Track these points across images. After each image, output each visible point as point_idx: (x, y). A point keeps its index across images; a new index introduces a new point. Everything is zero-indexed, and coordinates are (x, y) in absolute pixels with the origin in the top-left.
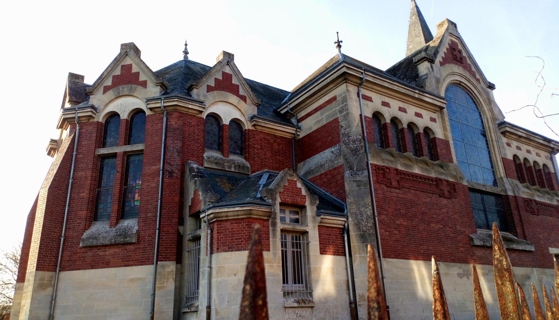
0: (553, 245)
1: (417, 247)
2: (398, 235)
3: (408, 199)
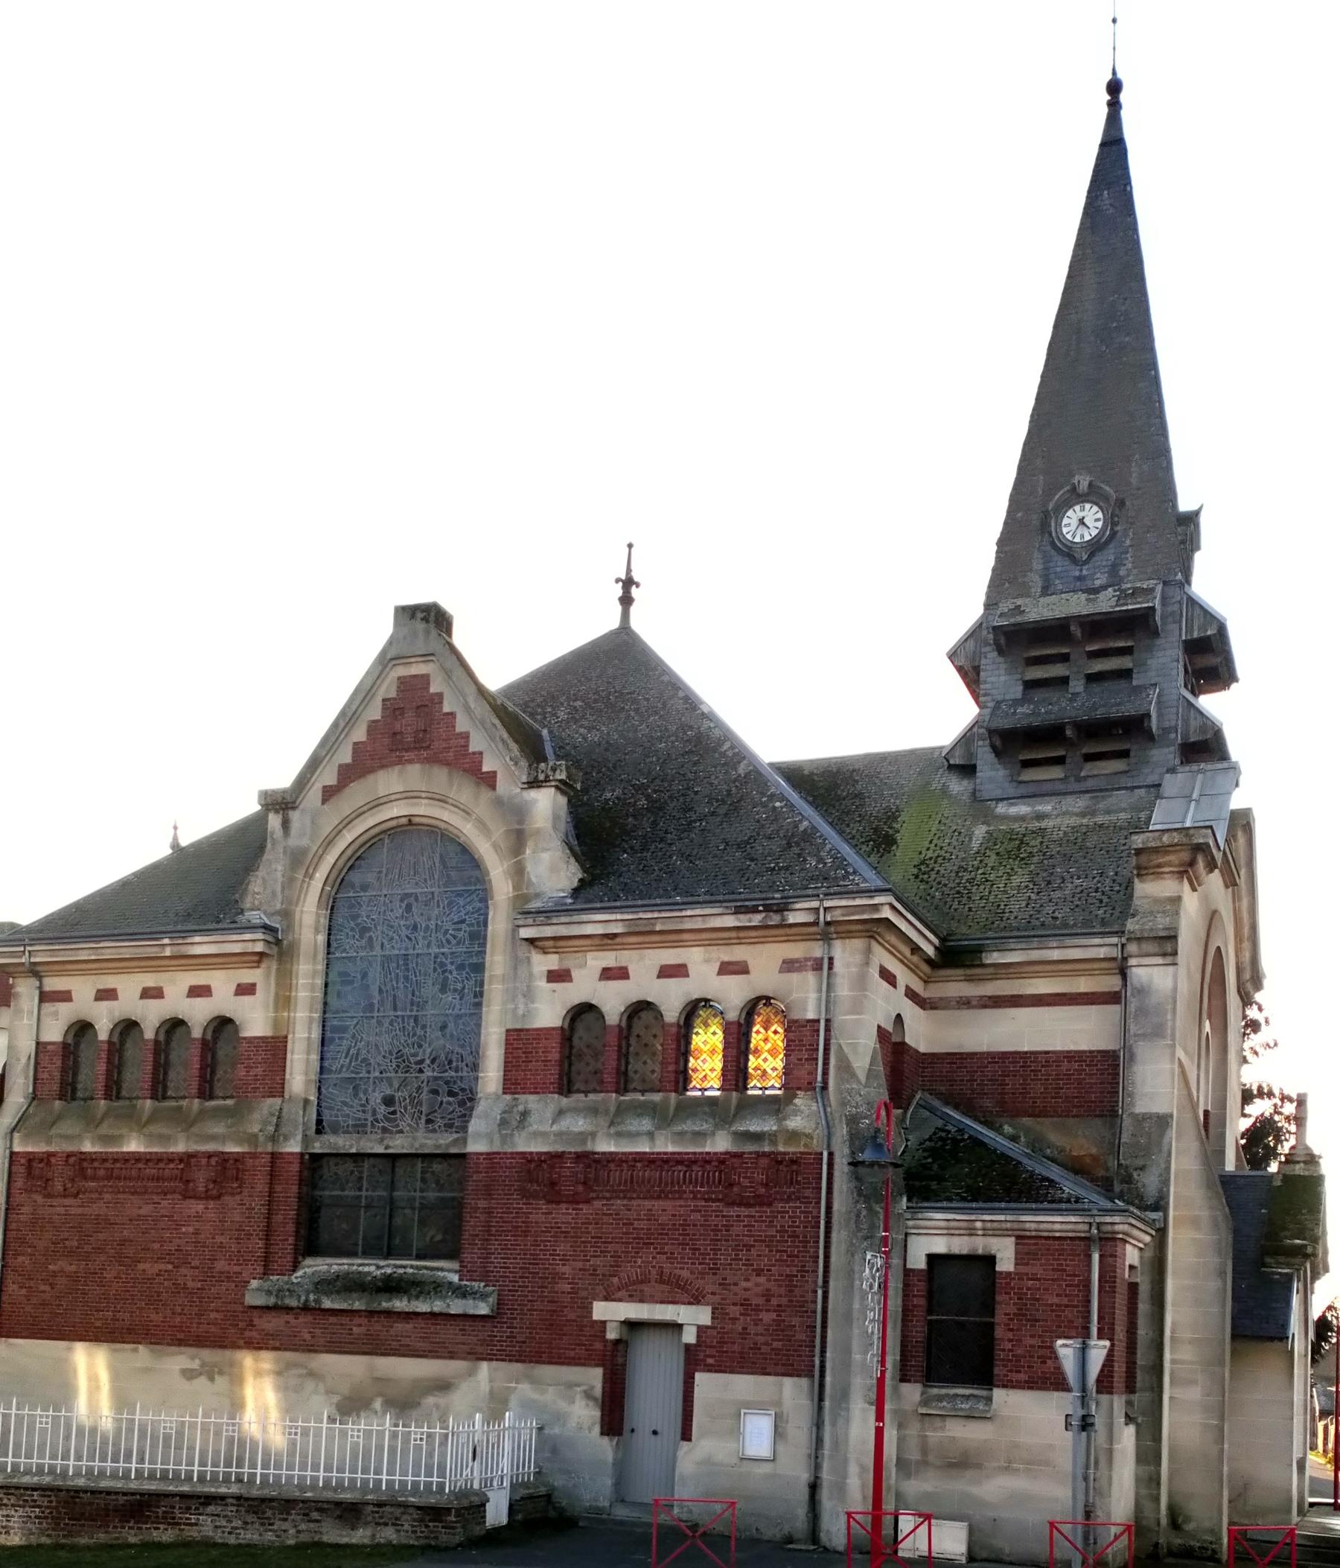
0: (620, 1294)
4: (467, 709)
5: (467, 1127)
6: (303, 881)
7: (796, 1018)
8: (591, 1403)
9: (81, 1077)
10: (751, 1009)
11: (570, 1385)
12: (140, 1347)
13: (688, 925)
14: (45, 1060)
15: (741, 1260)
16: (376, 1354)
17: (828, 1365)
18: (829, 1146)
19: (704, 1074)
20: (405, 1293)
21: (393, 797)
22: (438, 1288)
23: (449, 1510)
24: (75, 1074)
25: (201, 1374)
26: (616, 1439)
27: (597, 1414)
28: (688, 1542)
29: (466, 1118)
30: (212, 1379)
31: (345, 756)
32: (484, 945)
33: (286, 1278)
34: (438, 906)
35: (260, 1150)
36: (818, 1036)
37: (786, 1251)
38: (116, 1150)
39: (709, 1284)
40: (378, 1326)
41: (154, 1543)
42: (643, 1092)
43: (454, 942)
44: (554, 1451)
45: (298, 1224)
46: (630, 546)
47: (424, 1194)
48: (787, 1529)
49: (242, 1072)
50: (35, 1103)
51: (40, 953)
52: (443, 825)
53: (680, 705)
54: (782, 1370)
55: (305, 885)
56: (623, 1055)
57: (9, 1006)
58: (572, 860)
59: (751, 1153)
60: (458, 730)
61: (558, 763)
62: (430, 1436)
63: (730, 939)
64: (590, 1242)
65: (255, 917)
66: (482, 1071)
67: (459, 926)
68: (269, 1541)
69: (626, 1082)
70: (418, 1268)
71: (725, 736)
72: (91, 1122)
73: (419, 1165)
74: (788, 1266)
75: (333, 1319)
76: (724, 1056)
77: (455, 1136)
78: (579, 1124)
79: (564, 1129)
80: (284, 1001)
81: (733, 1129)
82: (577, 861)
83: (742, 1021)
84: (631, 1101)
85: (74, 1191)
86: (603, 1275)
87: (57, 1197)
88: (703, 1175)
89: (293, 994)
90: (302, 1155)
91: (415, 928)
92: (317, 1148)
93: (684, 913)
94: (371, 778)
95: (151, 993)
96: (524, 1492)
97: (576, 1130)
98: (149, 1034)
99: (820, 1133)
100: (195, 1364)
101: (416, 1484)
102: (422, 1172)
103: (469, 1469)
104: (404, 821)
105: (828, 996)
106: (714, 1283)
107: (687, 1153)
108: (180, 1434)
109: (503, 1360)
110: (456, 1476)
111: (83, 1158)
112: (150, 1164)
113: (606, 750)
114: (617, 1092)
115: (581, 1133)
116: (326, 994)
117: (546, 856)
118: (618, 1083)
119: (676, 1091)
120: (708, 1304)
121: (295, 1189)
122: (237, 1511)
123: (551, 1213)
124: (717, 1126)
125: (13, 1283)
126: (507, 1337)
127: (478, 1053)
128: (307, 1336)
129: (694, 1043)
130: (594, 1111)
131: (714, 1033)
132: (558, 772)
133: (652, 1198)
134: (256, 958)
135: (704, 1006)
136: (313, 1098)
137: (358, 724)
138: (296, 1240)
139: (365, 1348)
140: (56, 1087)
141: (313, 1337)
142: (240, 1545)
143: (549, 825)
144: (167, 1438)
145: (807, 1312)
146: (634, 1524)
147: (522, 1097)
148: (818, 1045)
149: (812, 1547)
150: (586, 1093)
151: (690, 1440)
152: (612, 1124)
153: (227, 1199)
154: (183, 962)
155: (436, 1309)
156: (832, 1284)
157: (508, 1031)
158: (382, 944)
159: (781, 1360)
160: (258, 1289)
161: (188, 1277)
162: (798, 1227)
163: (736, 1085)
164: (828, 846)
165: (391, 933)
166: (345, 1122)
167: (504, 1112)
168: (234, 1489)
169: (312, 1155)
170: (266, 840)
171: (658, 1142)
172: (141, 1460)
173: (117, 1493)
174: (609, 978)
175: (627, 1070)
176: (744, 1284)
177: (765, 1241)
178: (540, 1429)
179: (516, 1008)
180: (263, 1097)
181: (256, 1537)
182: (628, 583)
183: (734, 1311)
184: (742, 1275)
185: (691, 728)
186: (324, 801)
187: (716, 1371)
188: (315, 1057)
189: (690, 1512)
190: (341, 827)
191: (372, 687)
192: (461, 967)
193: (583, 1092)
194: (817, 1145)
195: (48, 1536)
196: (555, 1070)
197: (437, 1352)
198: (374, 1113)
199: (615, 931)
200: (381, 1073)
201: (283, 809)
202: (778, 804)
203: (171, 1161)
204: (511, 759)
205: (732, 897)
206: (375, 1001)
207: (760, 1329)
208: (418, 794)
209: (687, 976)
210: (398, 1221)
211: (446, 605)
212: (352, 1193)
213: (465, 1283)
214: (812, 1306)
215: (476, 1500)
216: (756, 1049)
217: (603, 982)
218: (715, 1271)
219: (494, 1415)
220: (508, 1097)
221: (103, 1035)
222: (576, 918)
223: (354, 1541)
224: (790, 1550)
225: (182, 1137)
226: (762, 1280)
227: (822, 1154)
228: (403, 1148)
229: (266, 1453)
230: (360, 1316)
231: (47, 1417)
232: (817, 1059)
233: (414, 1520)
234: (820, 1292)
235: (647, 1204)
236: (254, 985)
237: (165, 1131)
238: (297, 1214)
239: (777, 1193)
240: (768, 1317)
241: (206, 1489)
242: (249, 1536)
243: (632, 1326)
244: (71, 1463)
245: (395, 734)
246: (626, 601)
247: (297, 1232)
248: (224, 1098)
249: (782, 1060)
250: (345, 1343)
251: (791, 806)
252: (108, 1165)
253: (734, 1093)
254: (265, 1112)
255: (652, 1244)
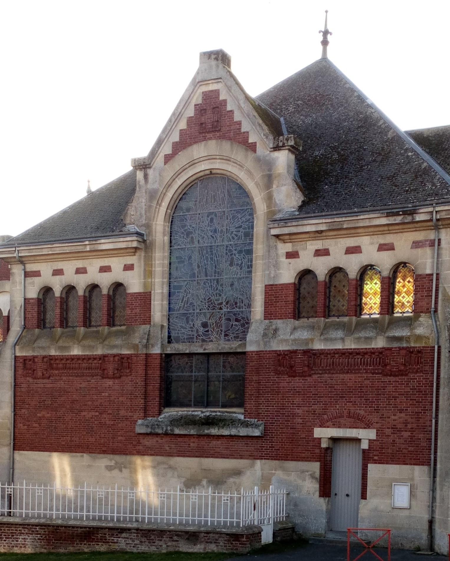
1: (58, 439)
2: (38, 428)
3: (57, 388)
4: (240, 107)
5: (246, 337)
6: (156, 208)
7: (420, 273)
8: (314, 481)
9: (48, 316)
10: (395, 270)
11: (303, 472)
12: (85, 455)
13: (361, 224)
14: (29, 307)
15: (391, 405)
16: (203, 457)
17: (438, 459)
18: (438, 343)
19: (370, 305)
20: (216, 425)
21: (202, 159)
22: (233, 422)
23: (242, 535)
24: (45, 315)
25: (115, 468)
26: (327, 499)
27: (317, 486)
28: (366, 550)
29: (245, 332)
30: (121, 471)
31: (176, 137)
32: (252, 239)
33: (156, 418)
34: (227, 219)
35: (139, 352)
36: (432, 283)
37: (416, 400)
38: (67, 354)
39: (374, 418)
40: (203, 442)
41: (97, 552)
42: (338, 316)
43: (236, 238)
44: (296, 505)
45: (160, 391)
46: (326, 12)
47: (225, 374)
48: (417, 543)
49: (128, 311)
50: (25, 330)
51: (23, 251)
52: (228, 174)
53: (355, 100)
54: (413, 461)
55: (157, 210)
56: (327, 297)
57: (9, 280)
58: (298, 190)
59: (396, 348)
60: (235, 120)
61: (289, 136)
62: (231, 498)
63: (384, 231)
64: (312, 397)
65: (132, 228)
66: (253, 308)
67: (238, 229)
68: (153, 551)
69: (329, 311)
70: (222, 412)
71: (380, 117)
72: (54, 340)
73: (222, 358)
74: (416, 407)
75: (180, 439)
76: (381, 296)
77: (240, 343)
78: (304, 335)
79: (297, 338)
80: (148, 273)
81: (386, 335)
82: (301, 190)
83: (391, 276)
84: (332, 322)
85: (47, 375)
86: (319, 414)
87: (38, 379)
88: (371, 360)
89: (153, 269)
90: (161, 354)
91: (215, 231)
92: (169, 351)
93: (359, 218)
94: (190, 149)
95: (81, 271)
96: (280, 526)
97: (303, 338)
98: (81, 293)
99: (434, 335)
100: (113, 463)
101: (225, 522)
102: (223, 362)
103: (252, 515)
104: (208, 172)
105: (438, 261)
106: (377, 417)
107: (363, 349)
108: (107, 498)
109: (268, 459)
110: (245, 518)
111: (51, 358)
112: (85, 361)
113: (315, 128)
114: (324, 317)
115: (306, 339)
116: (170, 268)
117: (284, 188)
118: (325, 312)
119: (356, 316)
120: (374, 428)
121: (158, 372)
122: (137, 536)
123: (291, 382)
124: (377, 334)
125: (20, 423)
126: (270, 447)
127: (250, 298)
128: (167, 448)
129: (365, 289)
130: (312, 328)
131: (376, 284)
132: (289, 141)
133: (344, 373)
134: (133, 250)
135: (370, 269)
136: (166, 324)
137: (182, 119)
138: (160, 399)
139: (197, 454)
140: (35, 322)
141: (170, 449)
142: (139, 553)
143: (285, 171)
144: (100, 500)
145: (427, 431)
146: (336, 542)
147: (274, 321)
148: (432, 288)
149: (430, 553)
150: (308, 318)
151: (366, 499)
152: (322, 334)
153: (123, 378)
154: (94, 254)
155: (233, 433)
156: (440, 416)
157: (266, 286)
158: (199, 241)
159: (413, 457)
160: (142, 425)
161: (106, 419)
162: (422, 386)
163: (388, 311)
164: (438, 176)
165: (203, 235)
166: (182, 336)
167: (265, 329)
168: (135, 525)
169: (166, 354)
170: (136, 186)
171: (346, 343)
172: (88, 511)
173: (77, 527)
174: (319, 255)
175: (329, 305)
176: (393, 417)
177: (403, 394)
178: (288, 494)
179: (270, 273)
180: (140, 324)
181: (147, 549)
182: (326, 33)
183: (388, 431)
184: (392, 412)
185: (361, 113)
186: (165, 163)
187: (379, 463)
188: (166, 303)
189: (367, 535)
190: (174, 177)
191: (188, 99)
192: (240, 252)
193: (307, 317)
194: (432, 342)
195: (45, 548)
196: (291, 306)
197: (234, 455)
198: (197, 331)
199: (322, 229)
200: (200, 310)
201: (144, 168)
202: (410, 154)
203: (95, 359)
204: (264, 135)
205: (386, 207)
206: (196, 272)
207: (402, 441)
208: (214, 157)
209: (361, 252)
210: (212, 388)
211: (228, 51)
212: (188, 374)
213: (247, 419)
214: (430, 428)
215: (256, 530)
216: (399, 291)
217: (315, 258)
218: (377, 410)
219: (264, 487)
220: (267, 321)
221: (57, 294)
222: (300, 223)
223: (195, 551)
224: (419, 554)
225: (100, 346)
226: (403, 415)
227: (434, 347)
228: (213, 350)
229: (150, 507)
230: (194, 438)
231: (41, 490)
232: (431, 296)
233: (225, 541)
234: (434, 421)
235: (341, 376)
236: (133, 265)
237: (92, 344)
238: (160, 386)
239: (410, 369)
240: (406, 434)
241: (121, 525)
242: (143, 548)
243: (335, 440)
244: (54, 512)
245: (202, 124)
246: (325, 43)
247: (160, 395)
248: (120, 325)
249: (412, 297)
250: (187, 451)
251: (417, 155)
252: (63, 362)
253: (387, 316)
254: (141, 332)
255: (345, 397)
